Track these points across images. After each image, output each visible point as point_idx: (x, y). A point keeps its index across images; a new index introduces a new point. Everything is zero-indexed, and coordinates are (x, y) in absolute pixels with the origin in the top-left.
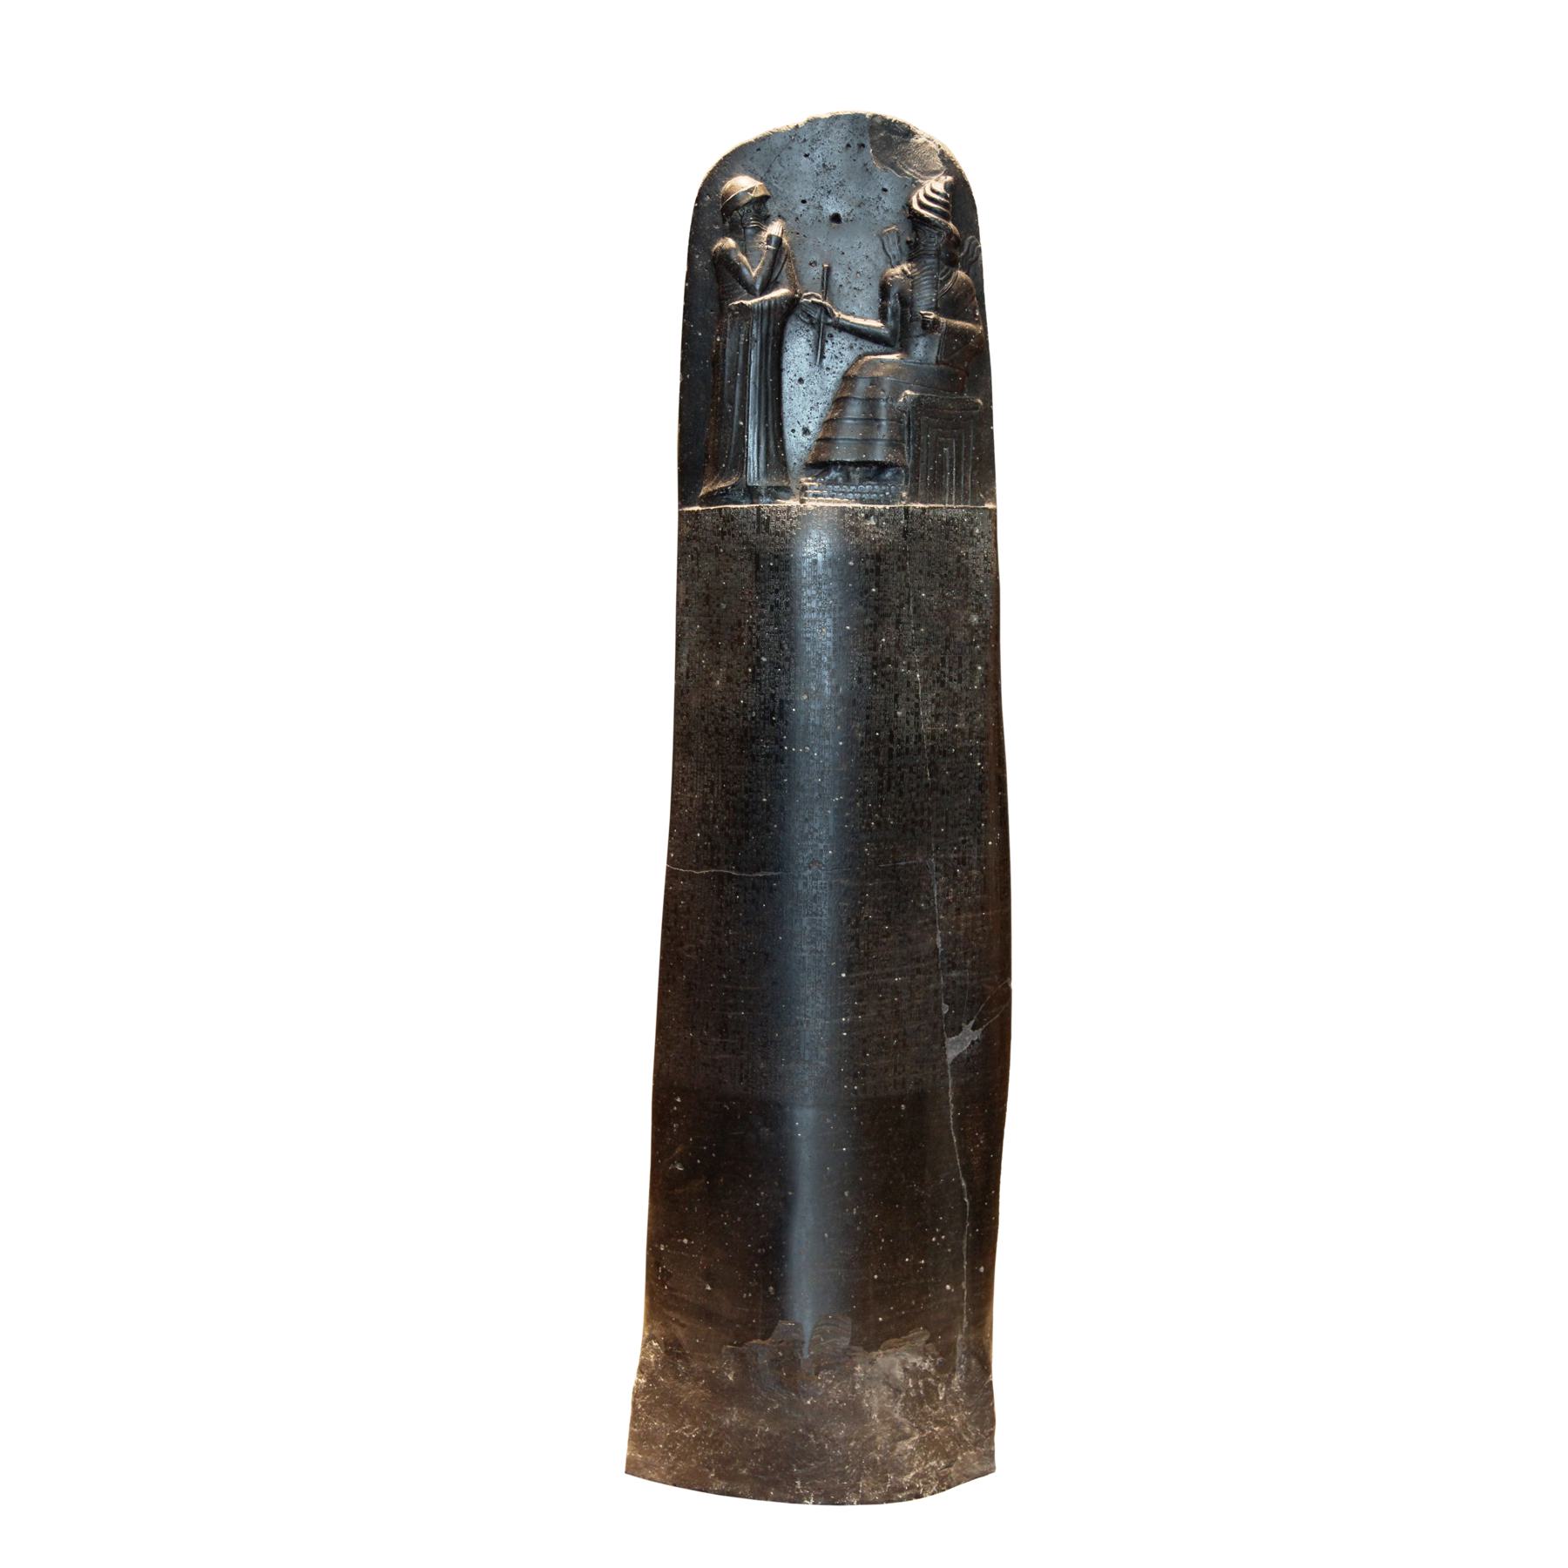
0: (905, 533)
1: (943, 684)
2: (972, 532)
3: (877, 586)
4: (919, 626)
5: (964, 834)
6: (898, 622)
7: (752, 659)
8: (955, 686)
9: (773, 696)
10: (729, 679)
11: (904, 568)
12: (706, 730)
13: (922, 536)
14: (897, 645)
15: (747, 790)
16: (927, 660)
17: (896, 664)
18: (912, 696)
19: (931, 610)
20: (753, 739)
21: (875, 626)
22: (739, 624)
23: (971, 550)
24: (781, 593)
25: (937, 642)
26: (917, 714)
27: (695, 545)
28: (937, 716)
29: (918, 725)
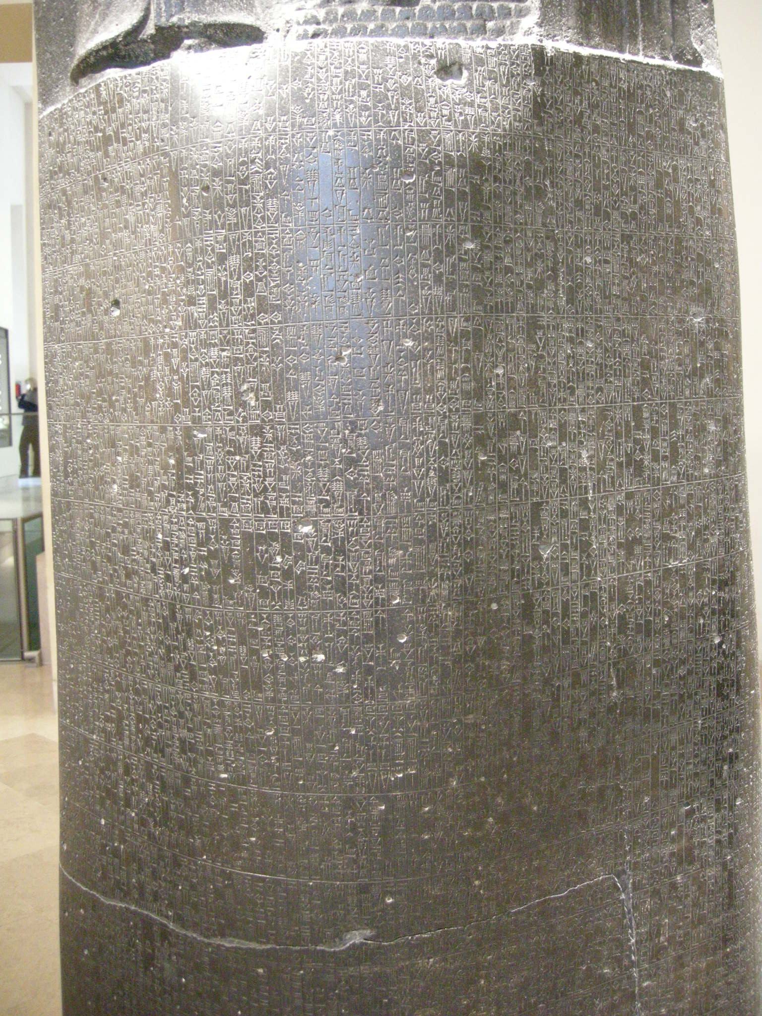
0: (539, 106)
1: (639, 468)
2: (681, 123)
3: (477, 233)
4: (582, 333)
5: (689, 798)
6: (533, 325)
7: (175, 435)
8: (667, 475)
9: (225, 524)
10: (134, 482)
11: (540, 193)
12: (101, 596)
13: (578, 120)
14: (532, 383)
15: (186, 747)
16: (603, 414)
17: (532, 430)
18: (573, 506)
19: (606, 297)
20: (189, 629)
21: (478, 338)
22: (147, 349)
23: (681, 162)
24: (234, 261)
25: (622, 374)
26: (585, 547)
27: (63, 183)
28: (629, 546)
29: (587, 571)
